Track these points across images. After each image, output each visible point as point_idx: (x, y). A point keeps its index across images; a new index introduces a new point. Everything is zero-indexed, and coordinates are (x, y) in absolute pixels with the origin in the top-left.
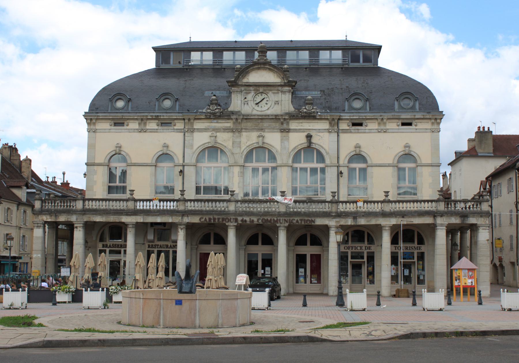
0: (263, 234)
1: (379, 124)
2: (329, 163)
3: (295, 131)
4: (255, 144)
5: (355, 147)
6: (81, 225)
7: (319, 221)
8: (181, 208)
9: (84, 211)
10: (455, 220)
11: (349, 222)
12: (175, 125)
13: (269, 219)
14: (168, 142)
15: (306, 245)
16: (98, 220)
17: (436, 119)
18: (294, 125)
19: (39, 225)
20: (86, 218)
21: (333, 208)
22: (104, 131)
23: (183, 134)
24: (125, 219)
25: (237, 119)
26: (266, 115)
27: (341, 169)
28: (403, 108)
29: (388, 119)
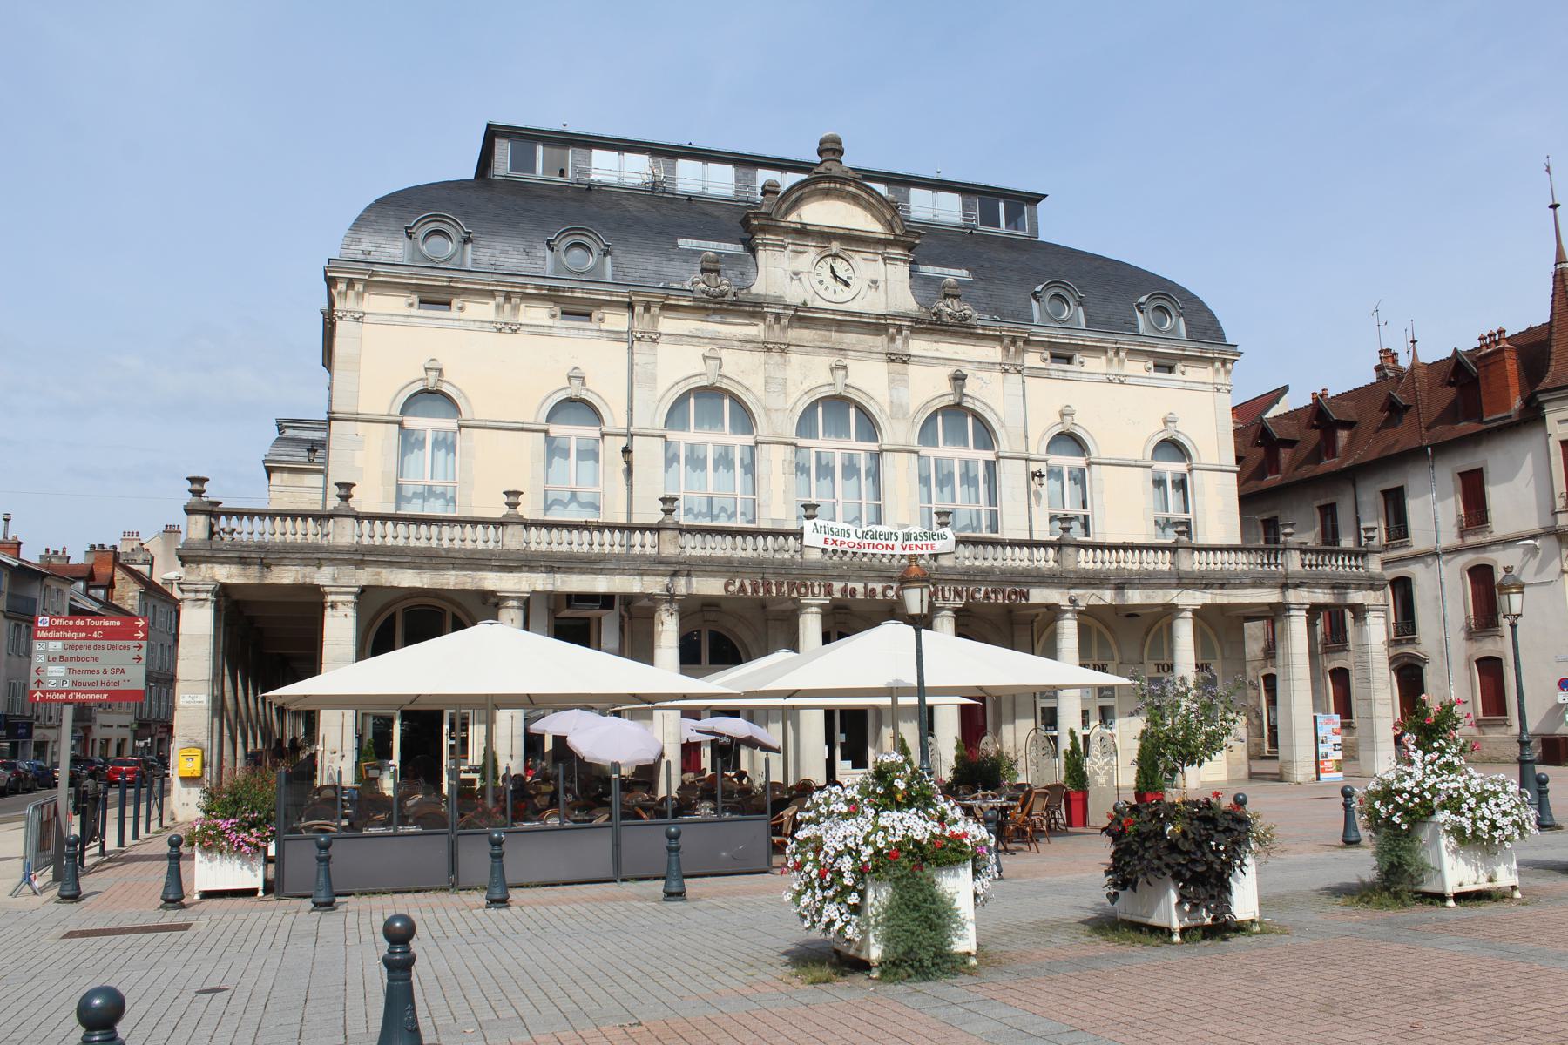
1: (1110, 361)
6: (351, 598)
7: (1038, 596)
9: (361, 557)
10: (1323, 596)
11: (1108, 597)
12: (602, 320)
14: (585, 369)
17: (1224, 362)
18: (918, 346)
19: (203, 596)
20: (365, 577)
22: (388, 319)
23: (626, 346)
25: (778, 318)
26: (853, 314)
27: (1034, 467)
29: (1130, 352)
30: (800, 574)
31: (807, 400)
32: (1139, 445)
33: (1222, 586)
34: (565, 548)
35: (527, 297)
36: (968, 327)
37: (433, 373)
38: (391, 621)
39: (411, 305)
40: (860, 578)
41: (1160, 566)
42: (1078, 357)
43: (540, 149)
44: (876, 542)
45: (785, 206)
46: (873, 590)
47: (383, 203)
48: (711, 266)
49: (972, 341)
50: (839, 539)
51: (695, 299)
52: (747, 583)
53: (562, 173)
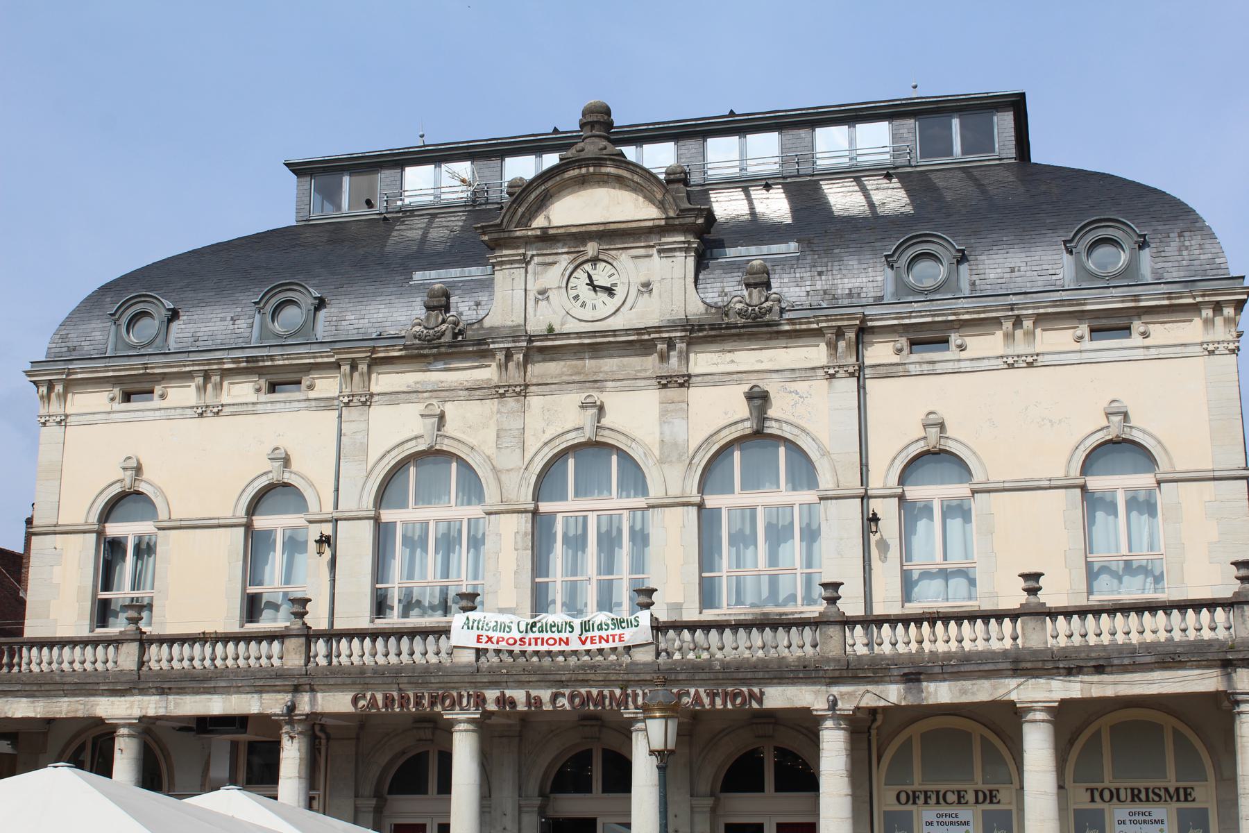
0: (604, 750)
1: (1009, 337)
2: (831, 486)
3: (713, 379)
4: (573, 435)
5: (925, 426)
7: (778, 697)
8: (295, 661)
11: (893, 694)
12: (311, 387)
13: (595, 692)
15: (760, 788)
16: (19, 715)
17: (1218, 307)
18: (703, 361)
21: (832, 644)
23: (336, 413)
24: (110, 708)
25: (509, 355)
26: (604, 333)
27: (875, 505)
28: (1093, 276)
29: (1039, 319)
30: (445, 683)
31: (548, 453)
32: (1060, 460)
33: (1099, 669)
34: (186, 664)
35: (225, 373)
36: (768, 324)
37: (129, 473)
38: (82, 748)
39: (113, 399)
40: (520, 684)
41: (995, 645)
42: (955, 339)
43: (346, 180)
44: (546, 636)
45: (521, 210)
46: (539, 701)
47: (106, 289)
48: (435, 302)
49: (783, 342)
50: (495, 635)
51: (405, 347)
52: (380, 697)
53: (369, 203)
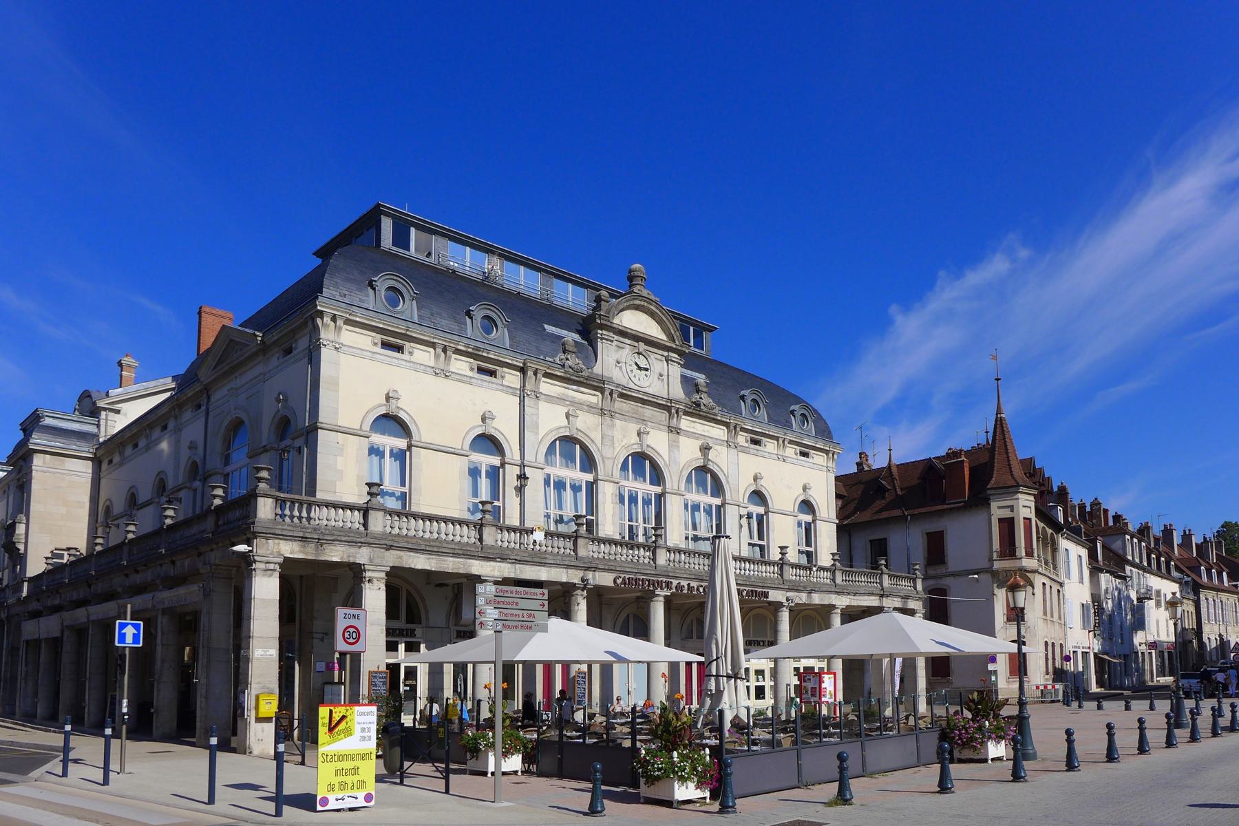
6: (383, 575)
9: (389, 543)
16: (419, 567)
18: (686, 423)
19: (271, 566)
20: (393, 558)
